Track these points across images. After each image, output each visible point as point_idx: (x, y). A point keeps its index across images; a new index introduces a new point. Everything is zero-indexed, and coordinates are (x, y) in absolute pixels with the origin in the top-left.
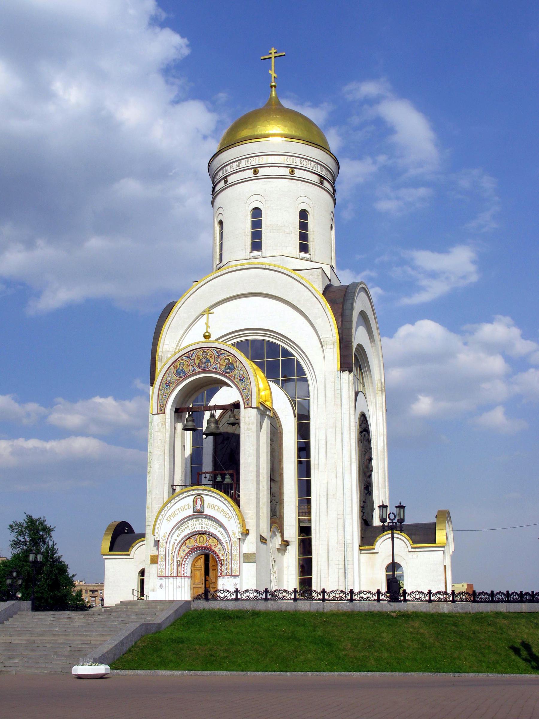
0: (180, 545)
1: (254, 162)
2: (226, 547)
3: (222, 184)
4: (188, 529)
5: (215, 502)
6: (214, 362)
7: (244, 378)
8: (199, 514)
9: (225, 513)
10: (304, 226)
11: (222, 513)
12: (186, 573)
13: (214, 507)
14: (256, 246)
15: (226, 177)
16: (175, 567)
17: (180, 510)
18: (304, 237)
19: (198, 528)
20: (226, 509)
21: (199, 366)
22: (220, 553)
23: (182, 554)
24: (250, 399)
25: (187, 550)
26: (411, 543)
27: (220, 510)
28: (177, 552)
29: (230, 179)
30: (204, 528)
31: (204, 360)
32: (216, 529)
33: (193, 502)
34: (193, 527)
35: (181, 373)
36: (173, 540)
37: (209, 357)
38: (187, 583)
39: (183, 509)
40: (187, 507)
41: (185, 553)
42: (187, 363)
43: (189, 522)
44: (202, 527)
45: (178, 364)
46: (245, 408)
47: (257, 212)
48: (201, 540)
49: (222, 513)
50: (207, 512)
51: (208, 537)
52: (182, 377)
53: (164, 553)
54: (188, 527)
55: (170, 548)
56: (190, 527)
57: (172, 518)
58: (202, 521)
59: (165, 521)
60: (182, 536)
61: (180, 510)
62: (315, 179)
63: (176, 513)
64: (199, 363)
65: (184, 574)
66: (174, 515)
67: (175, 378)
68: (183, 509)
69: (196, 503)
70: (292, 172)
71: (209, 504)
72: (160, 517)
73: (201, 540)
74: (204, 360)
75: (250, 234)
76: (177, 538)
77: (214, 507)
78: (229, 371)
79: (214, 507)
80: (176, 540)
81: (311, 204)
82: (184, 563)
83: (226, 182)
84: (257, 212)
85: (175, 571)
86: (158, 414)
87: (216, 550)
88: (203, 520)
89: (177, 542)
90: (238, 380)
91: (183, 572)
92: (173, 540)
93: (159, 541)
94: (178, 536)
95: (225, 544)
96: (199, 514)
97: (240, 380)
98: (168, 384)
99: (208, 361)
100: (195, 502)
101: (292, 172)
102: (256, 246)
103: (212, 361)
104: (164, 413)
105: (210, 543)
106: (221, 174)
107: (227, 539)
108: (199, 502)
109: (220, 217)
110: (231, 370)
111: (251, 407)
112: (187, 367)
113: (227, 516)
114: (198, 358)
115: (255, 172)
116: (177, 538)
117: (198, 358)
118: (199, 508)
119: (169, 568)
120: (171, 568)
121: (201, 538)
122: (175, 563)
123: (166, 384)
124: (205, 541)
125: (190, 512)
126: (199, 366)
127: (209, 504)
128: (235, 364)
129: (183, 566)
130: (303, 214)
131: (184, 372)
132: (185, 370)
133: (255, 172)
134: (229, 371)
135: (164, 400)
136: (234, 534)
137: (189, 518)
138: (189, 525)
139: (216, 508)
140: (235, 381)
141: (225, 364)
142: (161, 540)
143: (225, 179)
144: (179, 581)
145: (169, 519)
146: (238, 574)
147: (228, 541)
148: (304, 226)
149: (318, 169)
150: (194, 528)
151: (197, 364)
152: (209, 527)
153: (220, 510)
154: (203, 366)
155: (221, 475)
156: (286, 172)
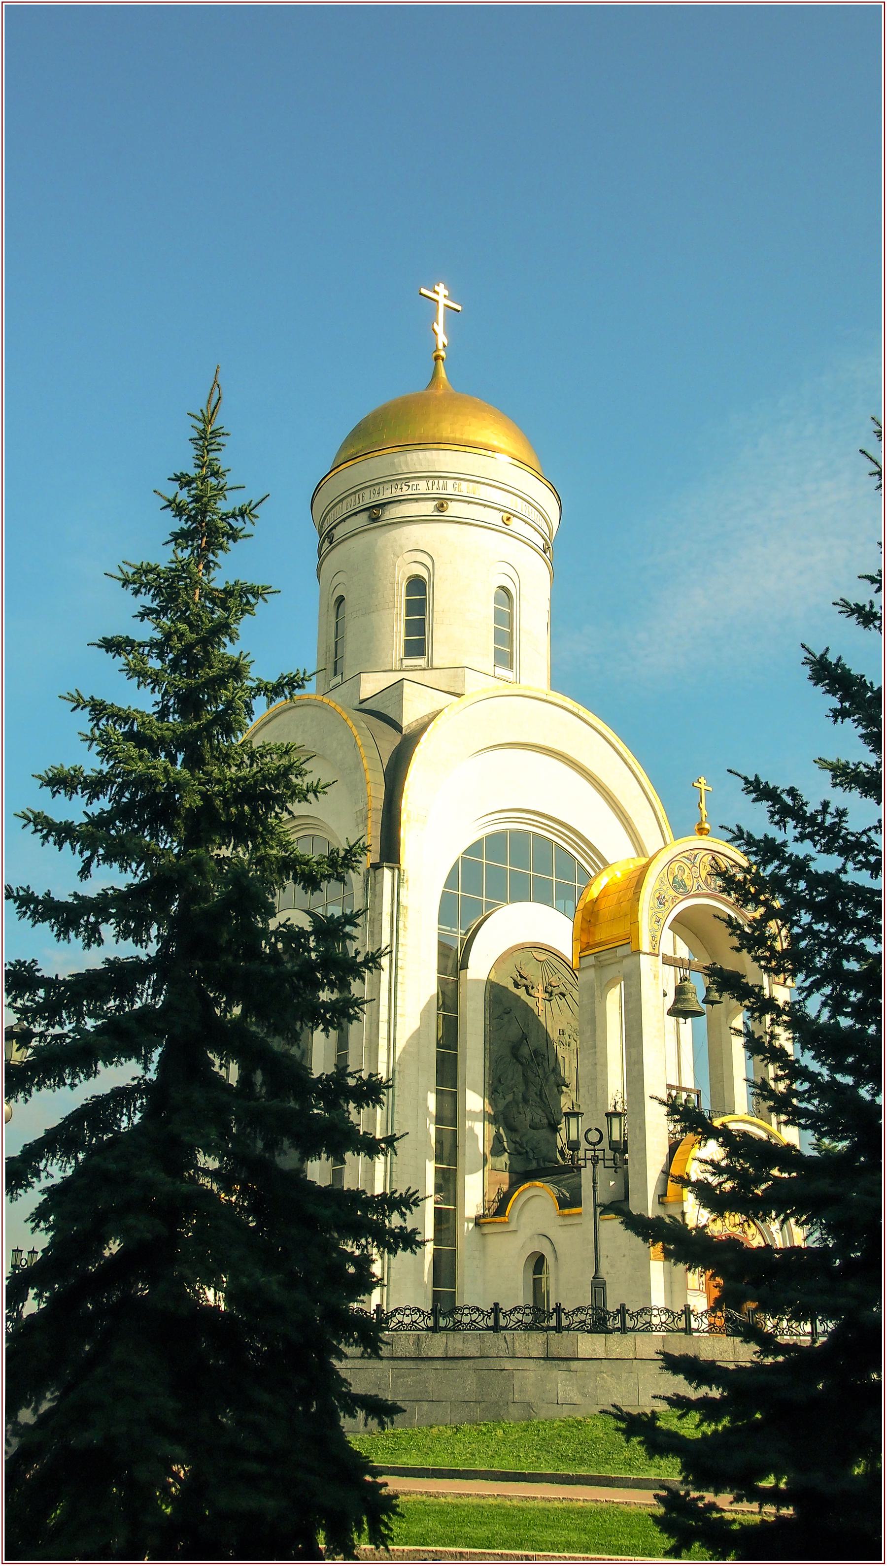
29: (454, 509)
52: (681, 894)
67: (672, 893)
83: (441, 508)
106: (435, 489)
115: (506, 521)
131: (685, 885)
133: (506, 521)
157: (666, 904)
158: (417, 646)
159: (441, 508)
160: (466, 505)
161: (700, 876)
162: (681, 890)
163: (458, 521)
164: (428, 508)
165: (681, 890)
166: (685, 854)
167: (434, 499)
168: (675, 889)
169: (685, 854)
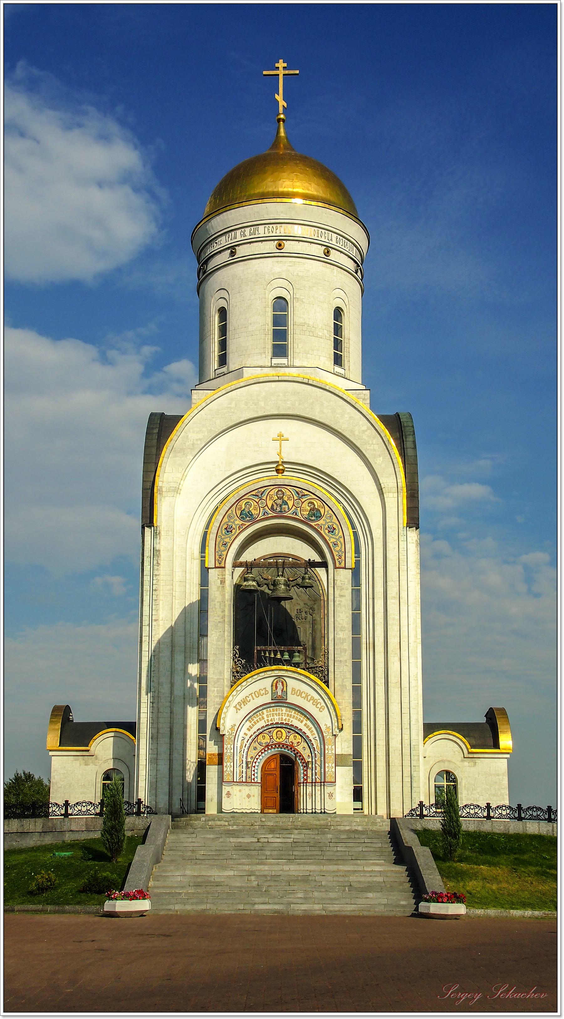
0: (250, 741)
1: (278, 231)
2: (315, 746)
3: (225, 256)
4: (263, 721)
5: (300, 687)
6: (294, 505)
7: (334, 529)
8: (279, 701)
9: (316, 703)
10: (338, 330)
11: (311, 701)
12: (257, 777)
13: (301, 694)
14: (280, 349)
15: (233, 247)
16: (244, 770)
17: (253, 695)
18: (338, 344)
19: (277, 719)
20: (317, 696)
21: (272, 509)
22: (306, 753)
23: (253, 753)
24: (343, 558)
25: (259, 748)
26: (469, 747)
27: (309, 698)
28: (246, 750)
29: (241, 251)
30: (285, 720)
31: (279, 502)
32: (302, 722)
33: (272, 686)
34: (270, 719)
35: (247, 516)
36: (242, 734)
37: (286, 498)
38: (256, 791)
39: (258, 694)
40: (264, 692)
41: (257, 751)
42: (256, 504)
43: (265, 711)
44: (282, 719)
45: (243, 503)
46: (335, 567)
47: (281, 304)
48: (279, 736)
49: (311, 701)
50: (291, 699)
51: (289, 732)
52: (248, 521)
53: (232, 751)
54: (263, 718)
55: (238, 744)
56: (266, 719)
57: (242, 706)
58: (282, 711)
59: (232, 710)
60: (255, 729)
61: (253, 695)
62: (351, 265)
63: (248, 699)
64: (273, 505)
65: (254, 779)
66: (244, 702)
67: (239, 522)
68: (258, 694)
69: (276, 688)
70: (327, 253)
71: (293, 689)
72: (227, 704)
73: (279, 736)
74: (279, 502)
75: (271, 332)
76: (247, 732)
77: (300, 694)
78: (313, 518)
79: (300, 694)
80: (245, 734)
81: (346, 301)
82: (254, 764)
83: (233, 254)
84: (281, 304)
85: (244, 775)
86: (216, 568)
87: (300, 748)
88: (284, 709)
89: (247, 738)
90: (327, 531)
91: (253, 777)
92: (242, 734)
93: (224, 735)
94: (249, 730)
95: (313, 741)
96: (279, 701)
97: (329, 532)
98: (229, 530)
99: (286, 503)
100: (274, 686)
101: (327, 253)
102: (280, 349)
103: (290, 503)
104: (224, 567)
105: (294, 739)
107: (316, 735)
108: (280, 686)
109: (223, 303)
110: (317, 517)
111: (345, 568)
112: (255, 509)
113: (319, 706)
114: (270, 498)
116: (247, 732)
117: (270, 498)
118: (280, 693)
119: (237, 770)
120: (240, 771)
121: (279, 733)
122: (244, 765)
123: (226, 529)
124: (284, 737)
125: (267, 699)
126: (272, 509)
127: (293, 689)
128: (322, 511)
129: (253, 769)
130: (338, 313)
131: (252, 515)
132: (253, 512)
134: (313, 518)
135: (224, 551)
136: (327, 728)
137: (265, 706)
138: (265, 716)
139: (303, 695)
140: (322, 532)
141: (309, 508)
142: (227, 734)
143: (233, 250)
144: (246, 789)
145: (238, 706)
146: (333, 780)
147: (317, 738)
148: (338, 330)
149: (354, 253)
150: (271, 720)
151: (270, 506)
152: (291, 719)
153: (309, 698)
154: (279, 509)
155: (288, 651)
156: (319, 251)
157: (234, 531)
158: (223, 360)
159: (233, 254)
160: (249, 245)
161: (267, 505)
162: (248, 519)
163: (244, 259)
164: (225, 256)
165: (248, 519)
166: (254, 493)
167: (228, 248)
168: (242, 519)
169: (254, 493)
